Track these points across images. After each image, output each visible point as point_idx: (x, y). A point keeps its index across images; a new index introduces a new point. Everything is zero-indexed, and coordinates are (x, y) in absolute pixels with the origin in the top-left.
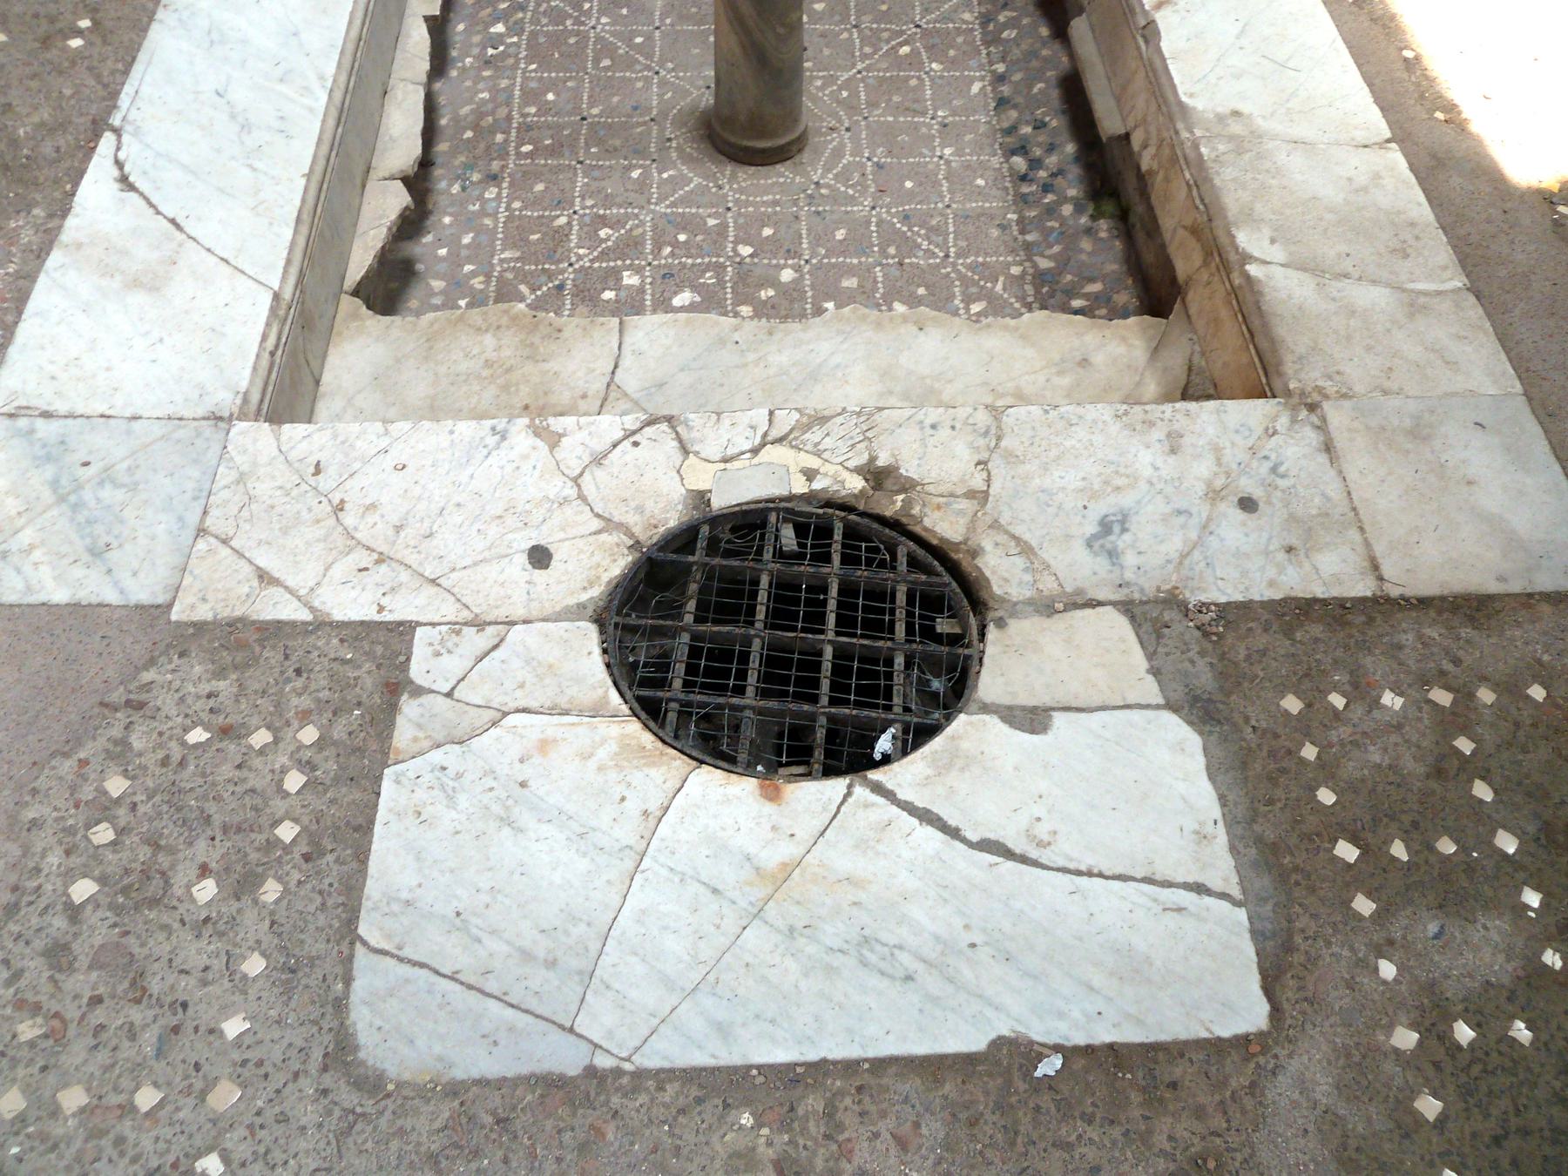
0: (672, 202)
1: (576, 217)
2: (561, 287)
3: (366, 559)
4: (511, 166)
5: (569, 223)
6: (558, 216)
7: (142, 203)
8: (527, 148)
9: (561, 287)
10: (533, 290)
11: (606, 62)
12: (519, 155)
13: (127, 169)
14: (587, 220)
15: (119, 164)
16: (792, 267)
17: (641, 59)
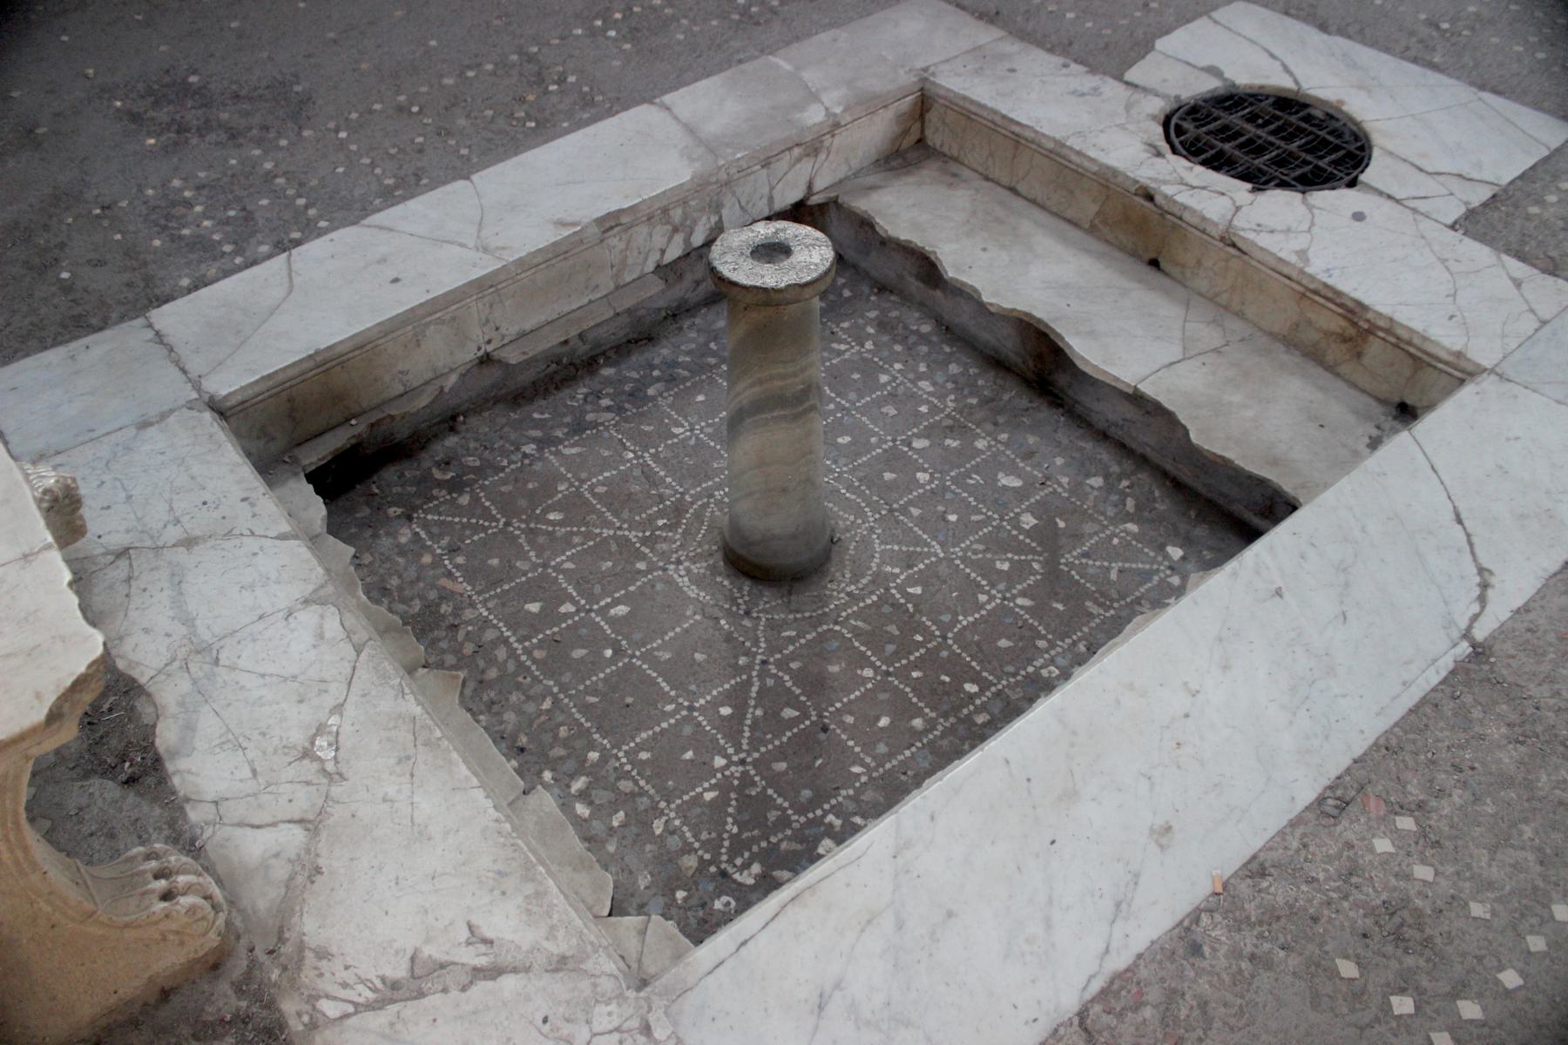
0: (917, 545)
1: (1008, 595)
2: (1086, 555)
3: (1451, 264)
4: (1004, 682)
5: (1023, 594)
6: (1022, 607)
7: (1477, 550)
8: (971, 688)
9: (1086, 555)
10: (1108, 569)
11: (789, 713)
12: (982, 691)
13: (1477, 591)
14: (1002, 586)
15: (1482, 599)
16: (909, 445)
17: (755, 689)
